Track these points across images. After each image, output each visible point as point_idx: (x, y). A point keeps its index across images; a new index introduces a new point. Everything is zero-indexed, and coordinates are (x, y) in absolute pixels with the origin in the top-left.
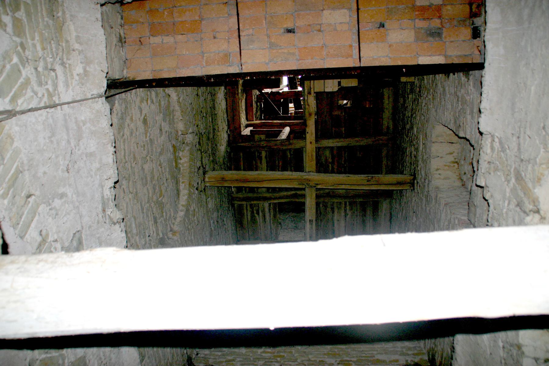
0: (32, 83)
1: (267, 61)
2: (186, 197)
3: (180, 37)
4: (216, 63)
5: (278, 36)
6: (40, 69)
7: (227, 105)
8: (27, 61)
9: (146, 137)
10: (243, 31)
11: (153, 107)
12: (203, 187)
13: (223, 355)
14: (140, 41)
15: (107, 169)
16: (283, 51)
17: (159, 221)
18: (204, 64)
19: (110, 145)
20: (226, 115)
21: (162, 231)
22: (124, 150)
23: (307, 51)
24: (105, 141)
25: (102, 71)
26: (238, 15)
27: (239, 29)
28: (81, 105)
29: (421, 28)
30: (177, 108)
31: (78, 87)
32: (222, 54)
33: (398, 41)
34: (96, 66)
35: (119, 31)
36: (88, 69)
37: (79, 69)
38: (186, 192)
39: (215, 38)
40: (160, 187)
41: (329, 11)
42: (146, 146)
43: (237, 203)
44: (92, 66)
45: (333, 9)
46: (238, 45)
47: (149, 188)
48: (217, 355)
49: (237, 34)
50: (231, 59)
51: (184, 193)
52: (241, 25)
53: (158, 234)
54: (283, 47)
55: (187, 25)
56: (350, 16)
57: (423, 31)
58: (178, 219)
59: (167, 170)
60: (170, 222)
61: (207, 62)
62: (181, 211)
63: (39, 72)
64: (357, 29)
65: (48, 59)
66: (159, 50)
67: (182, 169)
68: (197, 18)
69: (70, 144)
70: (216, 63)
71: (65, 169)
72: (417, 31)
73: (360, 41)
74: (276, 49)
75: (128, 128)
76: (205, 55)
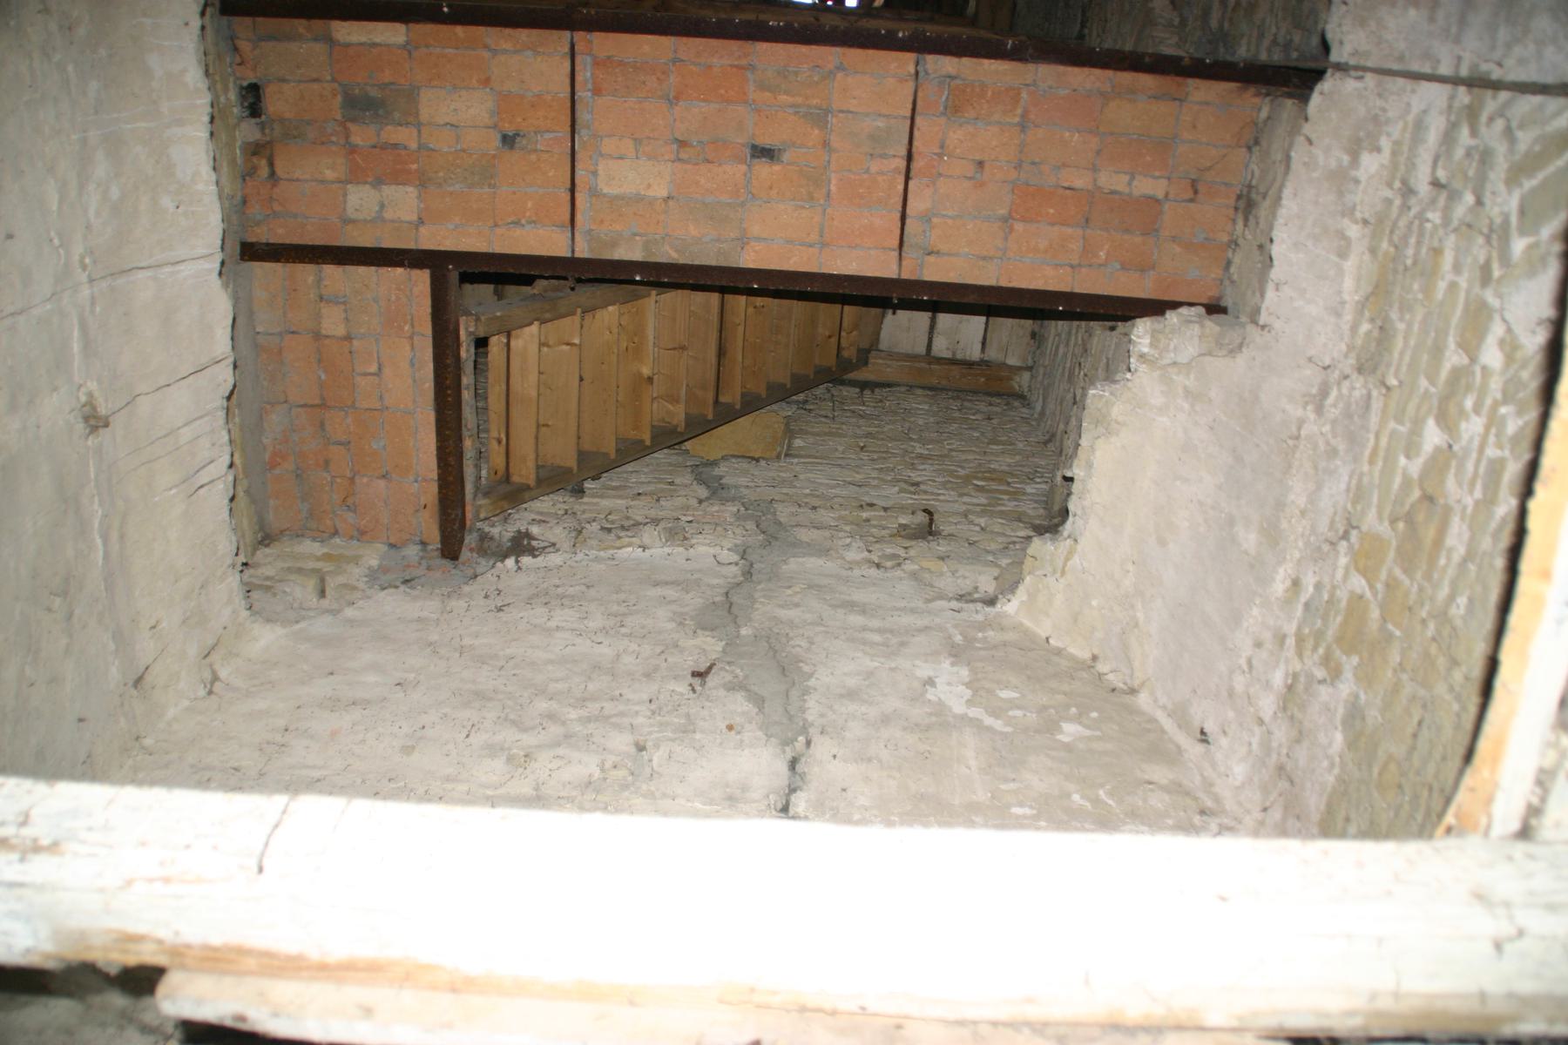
0: (1505, 166)
3: (1079, 183)
4: (990, 93)
5: (799, 142)
8: (1491, 230)
10: (896, 170)
14: (1196, 192)
16: (790, 100)
18: (1024, 95)
23: (722, 91)
25: (1310, 142)
27: (907, 179)
28: (1401, 58)
29: (401, 125)
32: (966, 115)
33: (463, 93)
35: (1247, 232)
36: (1346, 159)
39: (981, 164)
41: (650, 193)
45: (639, 199)
46: (916, 133)
49: (915, 165)
50: (944, 98)
52: (901, 187)
54: (791, 110)
55: (1052, 211)
56: (595, 173)
57: (397, 115)
61: (1016, 99)
64: (576, 136)
65: (1438, 221)
66: (1148, 158)
70: (990, 93)
72: (411, 118)
73: (569, 104)
74: (809, 106)
76: (1017, 120)
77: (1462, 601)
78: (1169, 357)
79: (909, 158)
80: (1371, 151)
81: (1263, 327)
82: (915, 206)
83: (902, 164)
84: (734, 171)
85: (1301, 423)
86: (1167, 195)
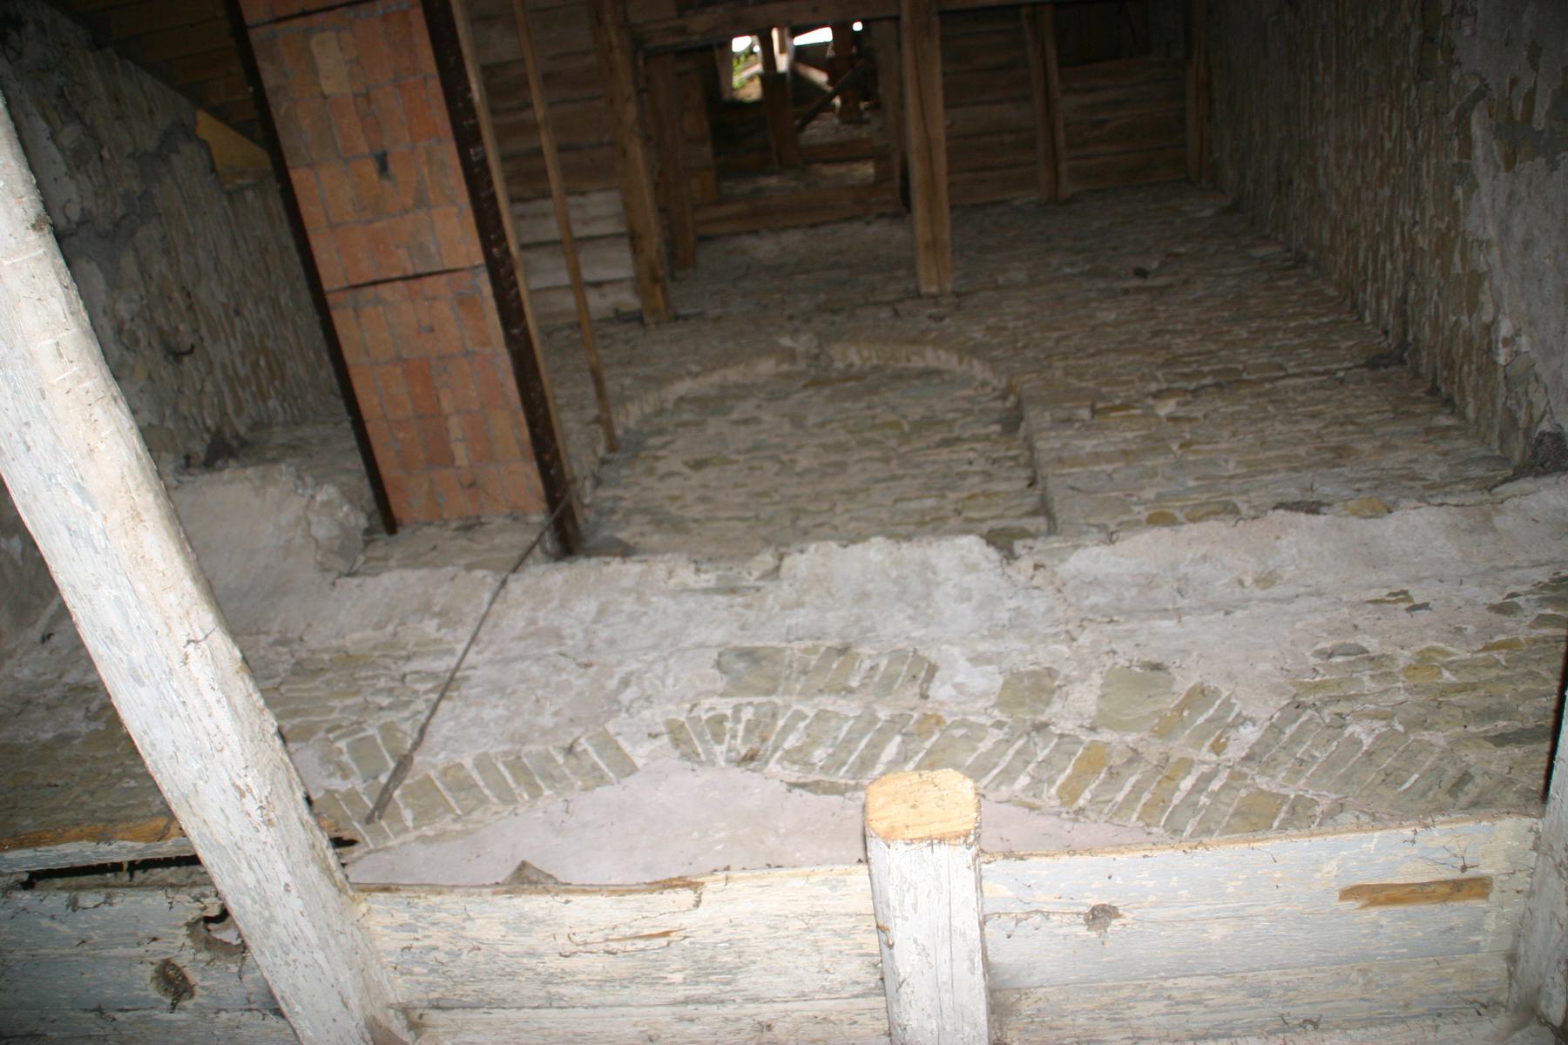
1: (455, 210)
2: (942, 354)
6: (385, 701)
7: (796, 227)
9: (736, 462)
11: (680, 444)
12: (953, 300)
13: (1392, 255)
17: (957, 432)
18: (488, 350)
19: (605, 570)
20: (823, 230)
21: (986, 425)
22: (729, 519)
24: (593, 578)
25: (452, 579)
26: (375, 283)
27: (405, 279)
30: (715, 378)
36: (436, 609)
38: (929, 353)
39: (432, 330)
40: (874, 427)
42: (756, 463)
43: (1068, 189)
47: (856, 457)
48: (1392, 275)
51: (932, 358)
52: (395, 275)
53: (987, 438)
58: (988, 375)
59: (848, 405)
60: (984, 399)
62: (971, 366)
67: (875, 362)
68: (398, 370)
71: (582, 670)
77: (133, 783)
78: (313, 518)
79: (417, 276)
81: (334, 584)
82: (385, 290)
83: (411, 272)
84: (362, 146)
85: (267, 633)
86: (459, 468)
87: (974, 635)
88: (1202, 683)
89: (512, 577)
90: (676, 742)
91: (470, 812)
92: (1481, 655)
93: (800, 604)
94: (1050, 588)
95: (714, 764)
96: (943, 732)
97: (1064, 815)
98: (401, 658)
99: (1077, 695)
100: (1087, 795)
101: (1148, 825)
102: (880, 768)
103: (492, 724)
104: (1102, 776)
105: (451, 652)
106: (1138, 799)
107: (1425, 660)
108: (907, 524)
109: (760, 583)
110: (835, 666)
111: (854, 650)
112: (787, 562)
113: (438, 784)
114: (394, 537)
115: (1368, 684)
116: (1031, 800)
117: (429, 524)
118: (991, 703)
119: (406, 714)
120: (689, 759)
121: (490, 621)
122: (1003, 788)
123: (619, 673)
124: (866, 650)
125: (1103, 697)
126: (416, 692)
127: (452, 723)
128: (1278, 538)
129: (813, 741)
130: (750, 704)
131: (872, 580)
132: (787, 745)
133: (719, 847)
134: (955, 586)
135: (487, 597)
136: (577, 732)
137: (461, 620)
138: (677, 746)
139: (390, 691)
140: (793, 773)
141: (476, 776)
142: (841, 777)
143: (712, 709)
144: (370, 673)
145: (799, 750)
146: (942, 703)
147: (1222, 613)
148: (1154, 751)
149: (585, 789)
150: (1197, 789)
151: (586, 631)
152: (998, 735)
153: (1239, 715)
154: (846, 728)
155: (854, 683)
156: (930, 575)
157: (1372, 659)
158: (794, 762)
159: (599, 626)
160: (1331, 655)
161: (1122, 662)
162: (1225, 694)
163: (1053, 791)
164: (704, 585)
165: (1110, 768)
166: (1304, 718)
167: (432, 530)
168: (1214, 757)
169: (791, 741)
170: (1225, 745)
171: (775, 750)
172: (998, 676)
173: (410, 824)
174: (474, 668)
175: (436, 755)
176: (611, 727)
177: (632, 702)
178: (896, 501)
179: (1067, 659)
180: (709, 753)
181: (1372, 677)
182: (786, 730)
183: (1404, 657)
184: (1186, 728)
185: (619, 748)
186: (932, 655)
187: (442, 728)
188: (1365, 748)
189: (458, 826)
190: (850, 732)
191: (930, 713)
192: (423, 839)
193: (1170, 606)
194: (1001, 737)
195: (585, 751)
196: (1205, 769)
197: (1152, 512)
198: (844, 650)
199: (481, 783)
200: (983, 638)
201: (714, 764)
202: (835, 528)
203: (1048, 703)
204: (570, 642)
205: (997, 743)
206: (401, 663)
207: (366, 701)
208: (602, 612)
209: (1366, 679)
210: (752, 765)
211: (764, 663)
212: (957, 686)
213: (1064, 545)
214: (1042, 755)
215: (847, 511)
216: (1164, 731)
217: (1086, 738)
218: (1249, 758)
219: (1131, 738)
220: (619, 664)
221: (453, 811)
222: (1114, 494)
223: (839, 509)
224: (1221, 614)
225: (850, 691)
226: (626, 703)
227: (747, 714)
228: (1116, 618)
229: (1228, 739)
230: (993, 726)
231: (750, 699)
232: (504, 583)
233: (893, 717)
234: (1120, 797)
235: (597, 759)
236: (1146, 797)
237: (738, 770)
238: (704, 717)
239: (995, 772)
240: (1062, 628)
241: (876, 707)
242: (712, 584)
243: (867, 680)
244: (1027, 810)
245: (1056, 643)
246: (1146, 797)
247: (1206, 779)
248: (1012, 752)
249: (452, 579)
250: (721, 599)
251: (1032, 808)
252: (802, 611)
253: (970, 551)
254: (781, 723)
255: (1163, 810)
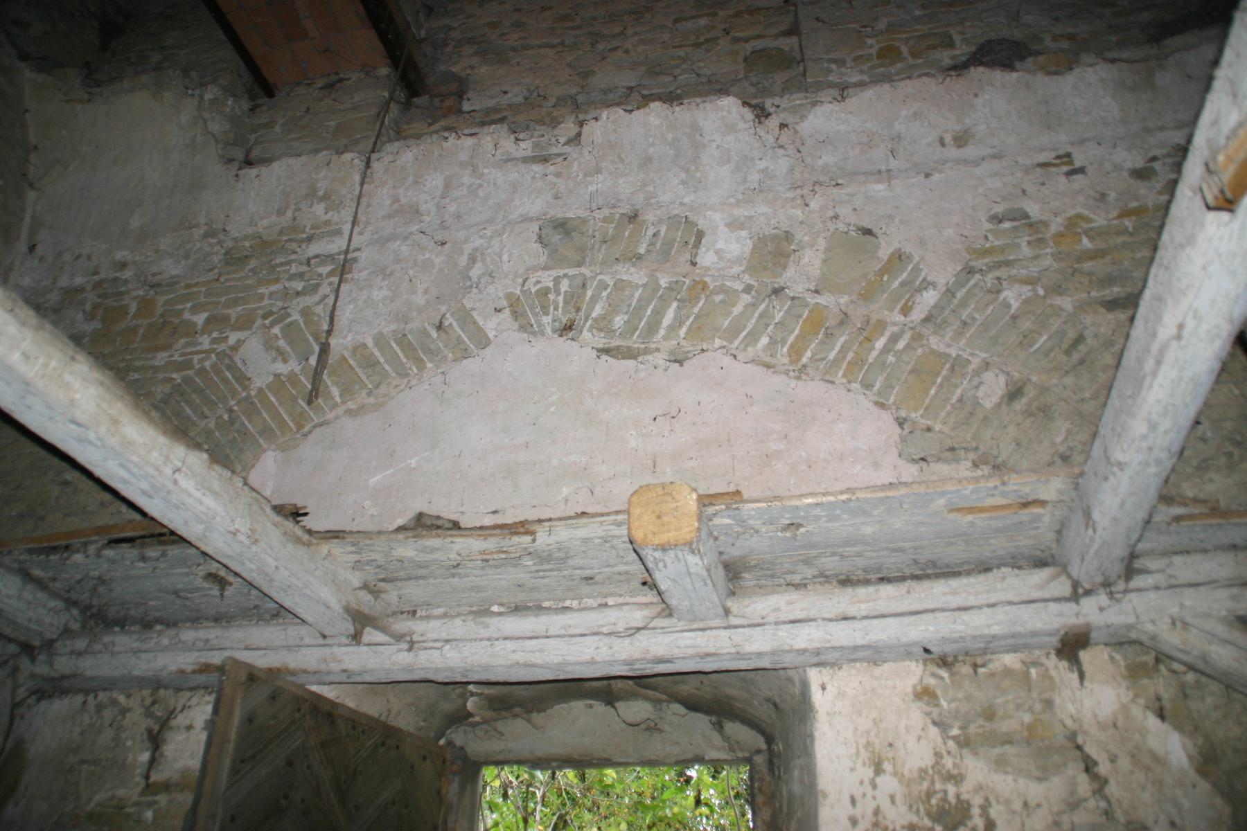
6: (299, 286)
15: (481, 151)
19: (445, 144)
22: (540, 47)
24: (436, 154)
31: (343, 212)
34: (321, 175)
36: (321, 193)
37: (319, 208)
44: (319, 185)
63: (304, 288)
65: (291, 272)
69: (411, 233)
71: (440, 248)
75: (504, 38)
77: (137, 376)
78: (206, 115)
80: (326, 208)
81: (237, 176)
85: (198, 226)
87: (732, 200)
88: (900, 249)
89: (374, 156)
90: (516, 315)
91: (378, 386)
92: (1116, 222)
93: (598, 171)
94: (791, 147)
95: (543, 335)
96: (707, 297)
97: (791, 374)
98: (303, 241)
99: (806, 260)
100: (809, 354)
101: (849, 382)
102: (662, 332)
103: (381, 305)
104: (820, 337)
105: (338, 232)
106: (844, 357)
107: (1073, 223)
108: (685, 46)
109: (567, 149)
110: (627, 234)
111: (641, 218)
112: (586, 129)
113: (351, 362)
114: (274, 100)
115: (1026, 251)
116: (768, 359)
117: (299, 84)
118: (742, 268)
119: (317, 298)
120: (525, 331)
121: (364, 200)
122: (750, 349)
123: (468, 249)
124: (650, 217)
125: (825, 261)
126: (320, 275)
127: (352, 306)
128: (976, 95)
129: (613, 309)
130: (566, 275)
131: (653, 145)
132: (594, 315)
133: (553, 409)
134: (718, 147)
135: (357, 178)
136: (444, 309)
137: (342, 202)
138: (516, 320)
139: (301, 276)
140: (601, 342)
141: (377, 353)
142: (635, 342)
143: (538, 282)
144: (283, 260)
145: (603, 317)
146: (708, 269)
147: (923, 175)
148: (858, 314)
149: (455, 360)
150: (886, 350)
151: (437, 206)
152: (746, 299)
153: (924, 279)
154: (637, 295)
155: (642, 251)
156: (698, 136)
157: (1031, 225)
158: (601, 330)
159: (447, 200)
160: (1000, 221)
161: (842, 227)
162: (917, 259)
163: (785, 350)
164: (524, 154)
165: (827, 328)
166: (972, 282)
167: (301, 90)
168: (902, 318)
169: (598, 311)
170: (911, 308)
171: (586, 320)
172: (748, 241)
173: (338, 399)
174: (359, 249)
175: (345, 337)
176: (468, 304)
177: (479, 278)
178: (676, 21)
179: (801, 223)
180: (540, 325)
181: (1029, 243)
182: (594, 300)
183: (1056, 225)
184: (884, 292)
185: (475, 323)
186: (702, 224)
187: (345, 314)
188: (1013, 311)
189: (372, 400)
190: (639, 301)
191: (698, 279)
192: (349, 412)
193: (883, 168)
194: (750, 300)
195: (451, 324)
196: (895, 329)
197: (883, 45)
198: (633, 217)
199: (382, 360)
200: (738, 203)
201: (543, 335)
202: (627, 51)
203: (785, 267)
204: (427, 219)
205: (746, 307)
206: (304, 246)
207: (285, 288)
208: (447, 186)
209: (1024, 245)
210: (570, 335)
211: (573, 234)
212: (718, 252)
213: (804, 101)
214: (779, 316)
215: (636, 33)
216: (867, 296)
217: (812, 300)
218: (928, 319)
219: (844, 300)
220: (466, 241)
221: (366, 385)
222: (853, 26)
223: (629, 32)
224: (921, 178)
225: (639, 257)
226: (475, 279)
227: (565, 286)
228: (840, 181)
229: (914, 303)
230: (743, 291)
231: (566, 271)
232: (368, 164)
233: (670, 283)
234: (832, 356)
235: (461, 333)
236: (850, 356)
237: (561, 340)
238: (533, 290)
239: (744, 333)
240: (799, 191)
241: (658, 275)
242: (529, 153)
243: (651, 247)
244: (765, 369)
245: (793, 207)
246: (850, 356)
247: (894, 339)
248: (756, 315)
249: (328, 164)
250: (537, 168)
251: (768, 366)
252: (601, 178)
253: (729, 112)
254: (589, 293)
255: (861, 370)
